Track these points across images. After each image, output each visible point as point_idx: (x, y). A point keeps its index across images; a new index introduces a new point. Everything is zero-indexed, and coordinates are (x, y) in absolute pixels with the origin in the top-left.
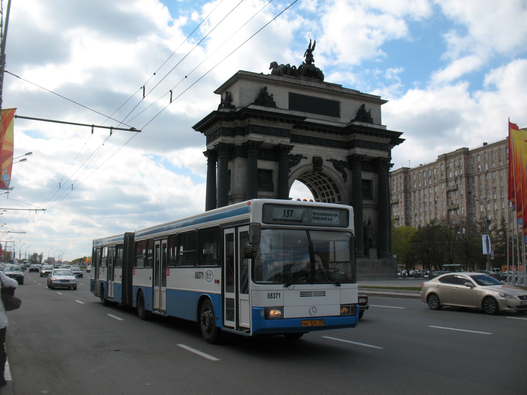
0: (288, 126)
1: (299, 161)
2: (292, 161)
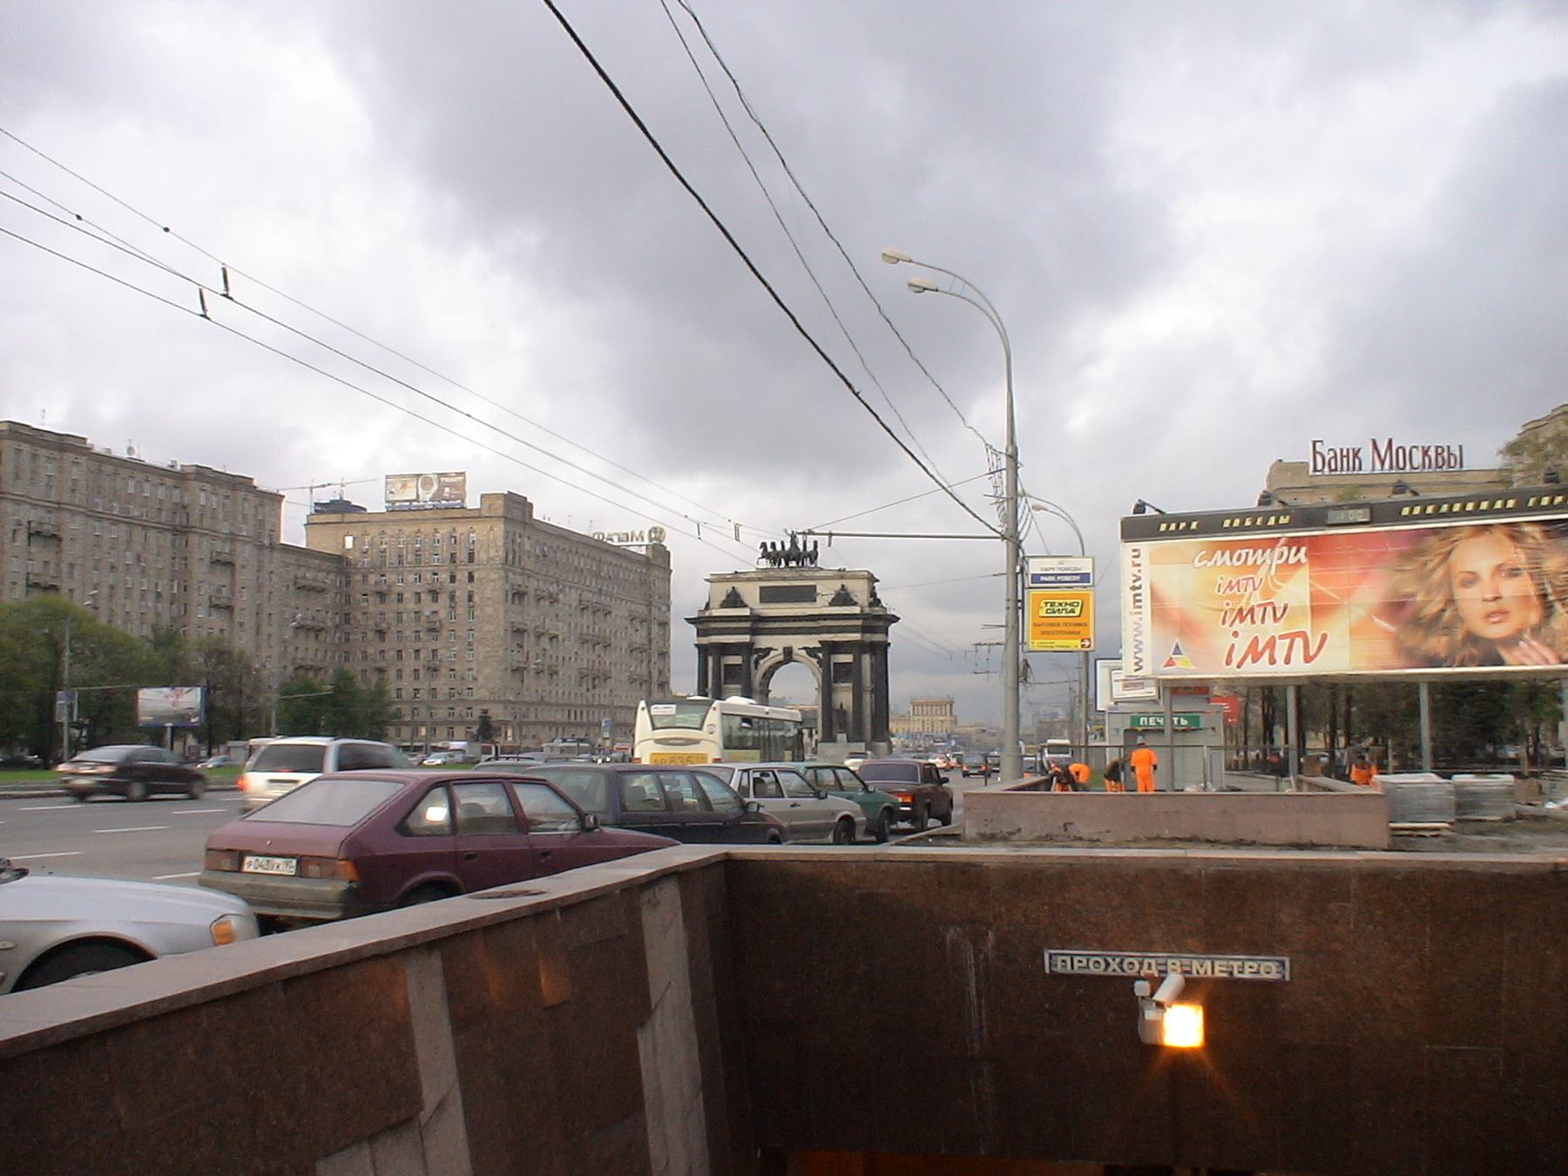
0: (747, 625)
1: (768, 654)
2: (761, 654)
